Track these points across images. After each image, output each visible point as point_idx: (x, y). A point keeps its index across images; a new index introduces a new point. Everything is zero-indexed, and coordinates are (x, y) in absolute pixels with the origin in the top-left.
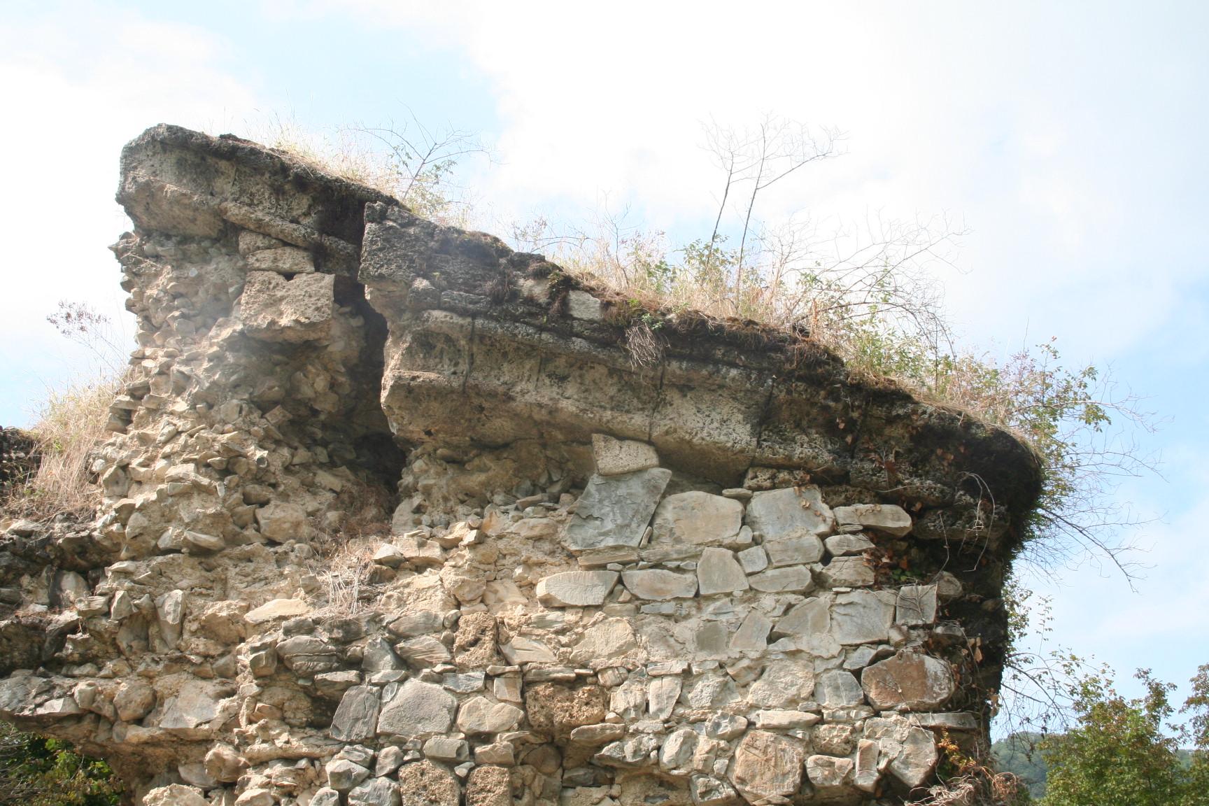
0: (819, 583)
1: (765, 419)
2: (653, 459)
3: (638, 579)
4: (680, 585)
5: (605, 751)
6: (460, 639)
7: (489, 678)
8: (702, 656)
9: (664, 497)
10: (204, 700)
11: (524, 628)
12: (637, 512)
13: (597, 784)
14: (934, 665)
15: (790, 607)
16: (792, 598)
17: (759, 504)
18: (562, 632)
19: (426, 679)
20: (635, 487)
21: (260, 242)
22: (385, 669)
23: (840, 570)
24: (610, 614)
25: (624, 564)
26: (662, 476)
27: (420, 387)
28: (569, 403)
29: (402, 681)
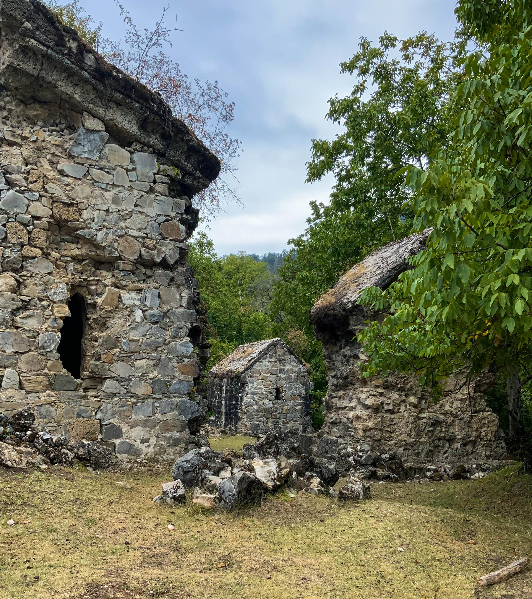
0: (151, 190)
1: (143, 125)
2: (104, 129)
3: (94, 172)
4: (108, 178)
5: (79, 232)
6: (30, 179)
7: (41, 196)
8: (113, 206)
9: (106, 143)
11: (53, 180)
12: (96, 147)
13: (73, 242)
16: (143, 193)
17: (136, 156)
19: (17, 191)
20: (96, 137)
23: (159, 187)
24: (84, 183)
25: (90, 165)
27: (20, 69)
29: (8, 190)
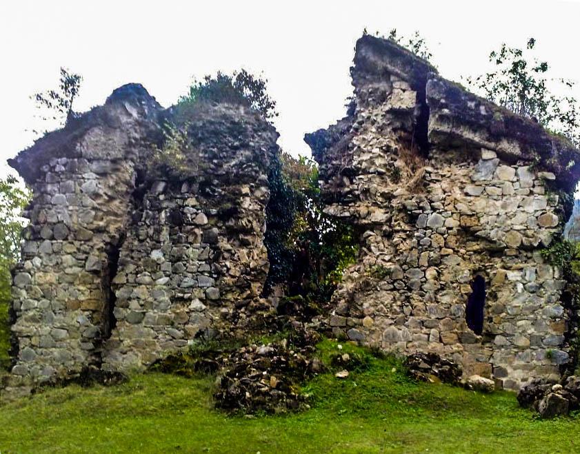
0: (531, 193)
3: (489, 189)
4: (498, 191)
5: (478, 233)
6: (446, 203)
7: (452, 213)
10: (381, 214)
14: (555, 217)
15: (524, 199)
18: (470, 202)
19: (438, 213)
20: (490, 164)
21: (396, 79)
22: (429, 211)
26: (498, 160)
28: (477, 138)
29: (432, 213)
